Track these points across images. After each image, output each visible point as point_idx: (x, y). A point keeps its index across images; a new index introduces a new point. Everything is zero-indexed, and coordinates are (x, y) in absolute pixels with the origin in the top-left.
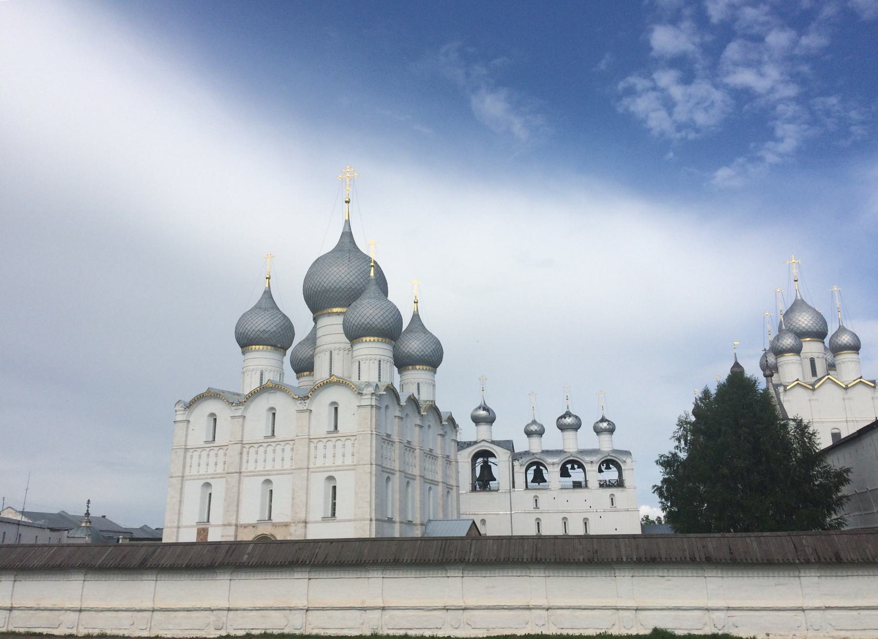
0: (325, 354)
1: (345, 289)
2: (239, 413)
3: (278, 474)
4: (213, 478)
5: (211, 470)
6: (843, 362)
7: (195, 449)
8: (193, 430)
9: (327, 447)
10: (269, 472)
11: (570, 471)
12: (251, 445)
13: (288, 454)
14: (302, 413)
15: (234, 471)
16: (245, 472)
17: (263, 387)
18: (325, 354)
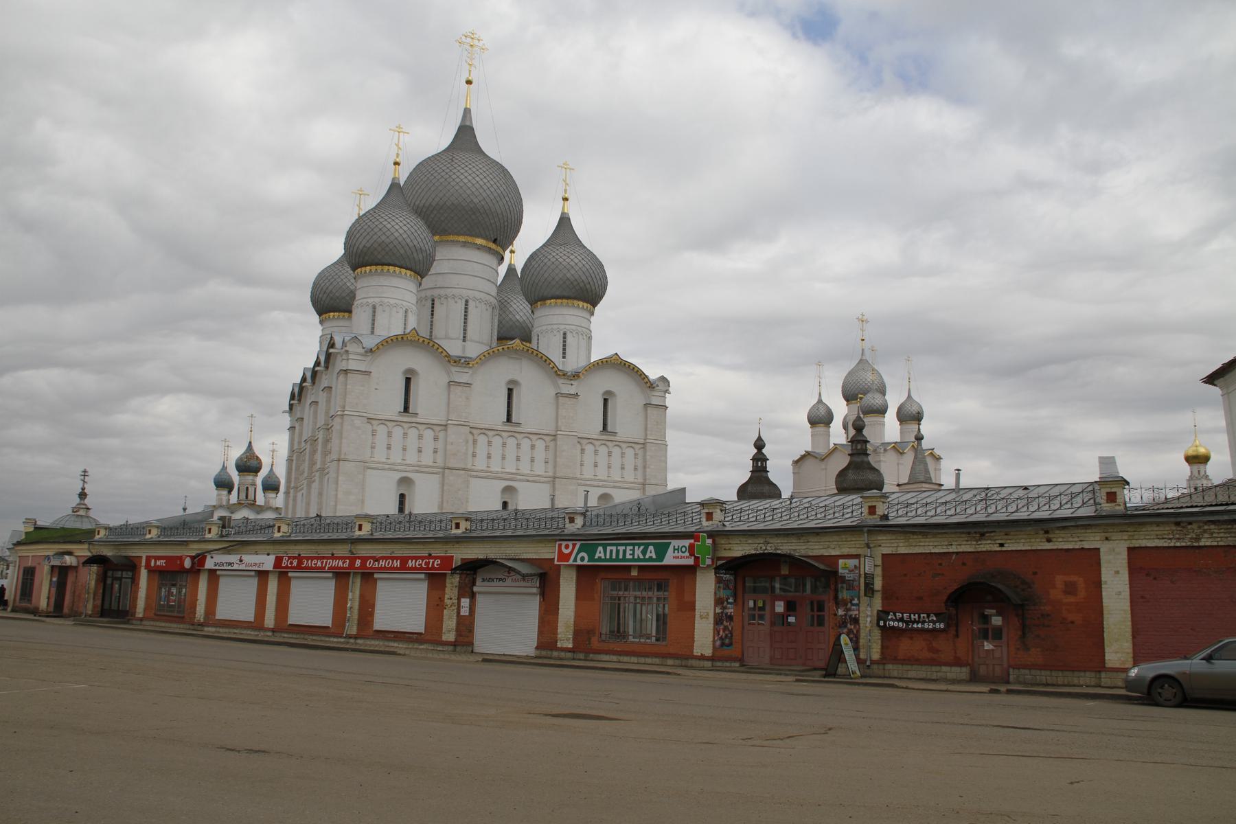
0: (456, 302)
3: (528, 481)
4: (417, 472)
5: (412, 458)
8: (376, 389)
9: (493, 444)
10: (512, 477)
13: (540, 453)
14: (567, 399)
16: (473, 470)
17: (508, 348)
18: (456, 302)
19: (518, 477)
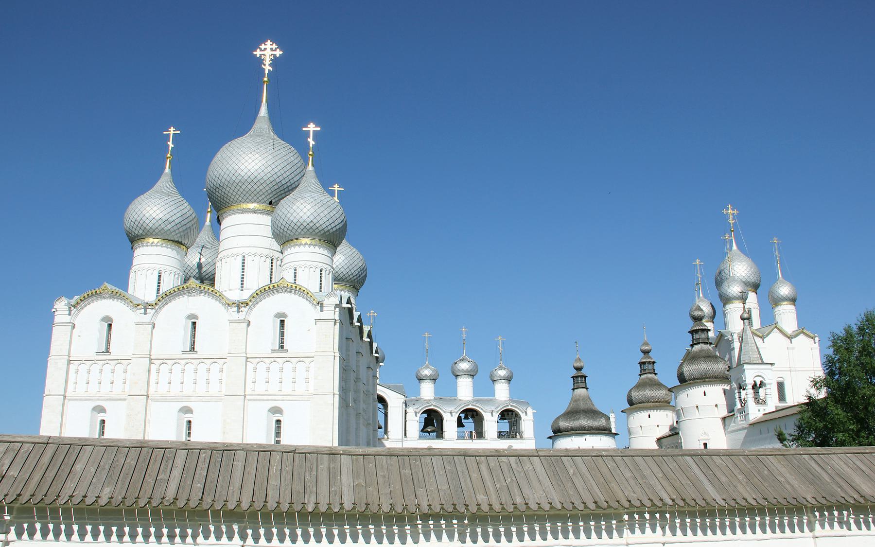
0: (235, 259)
1: (268, 182)
2: (147, 318)
3: (201, 401)
4: (107, 400)
5: (105, 389)
6: (783, 313)
7: (82, 361)
11: (463, 421)
12: (163, 360)
15: (139, 392)
18: (235, 259)
19: (193, 398)
